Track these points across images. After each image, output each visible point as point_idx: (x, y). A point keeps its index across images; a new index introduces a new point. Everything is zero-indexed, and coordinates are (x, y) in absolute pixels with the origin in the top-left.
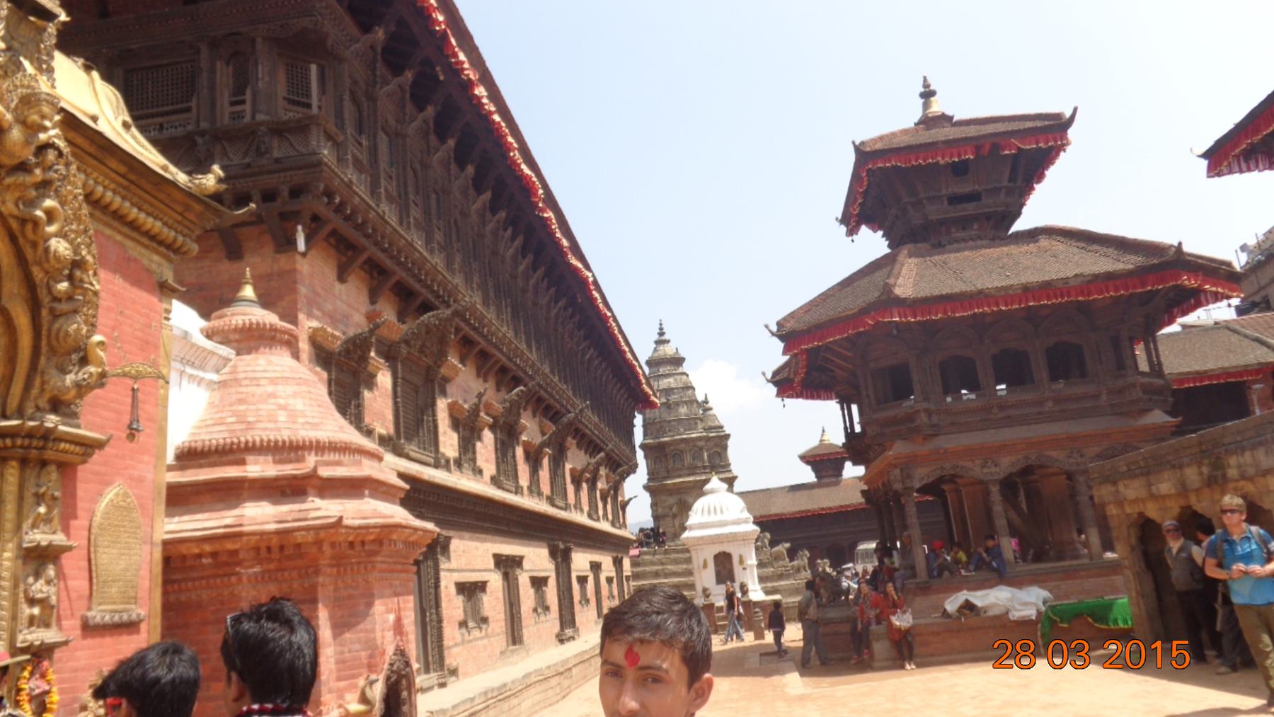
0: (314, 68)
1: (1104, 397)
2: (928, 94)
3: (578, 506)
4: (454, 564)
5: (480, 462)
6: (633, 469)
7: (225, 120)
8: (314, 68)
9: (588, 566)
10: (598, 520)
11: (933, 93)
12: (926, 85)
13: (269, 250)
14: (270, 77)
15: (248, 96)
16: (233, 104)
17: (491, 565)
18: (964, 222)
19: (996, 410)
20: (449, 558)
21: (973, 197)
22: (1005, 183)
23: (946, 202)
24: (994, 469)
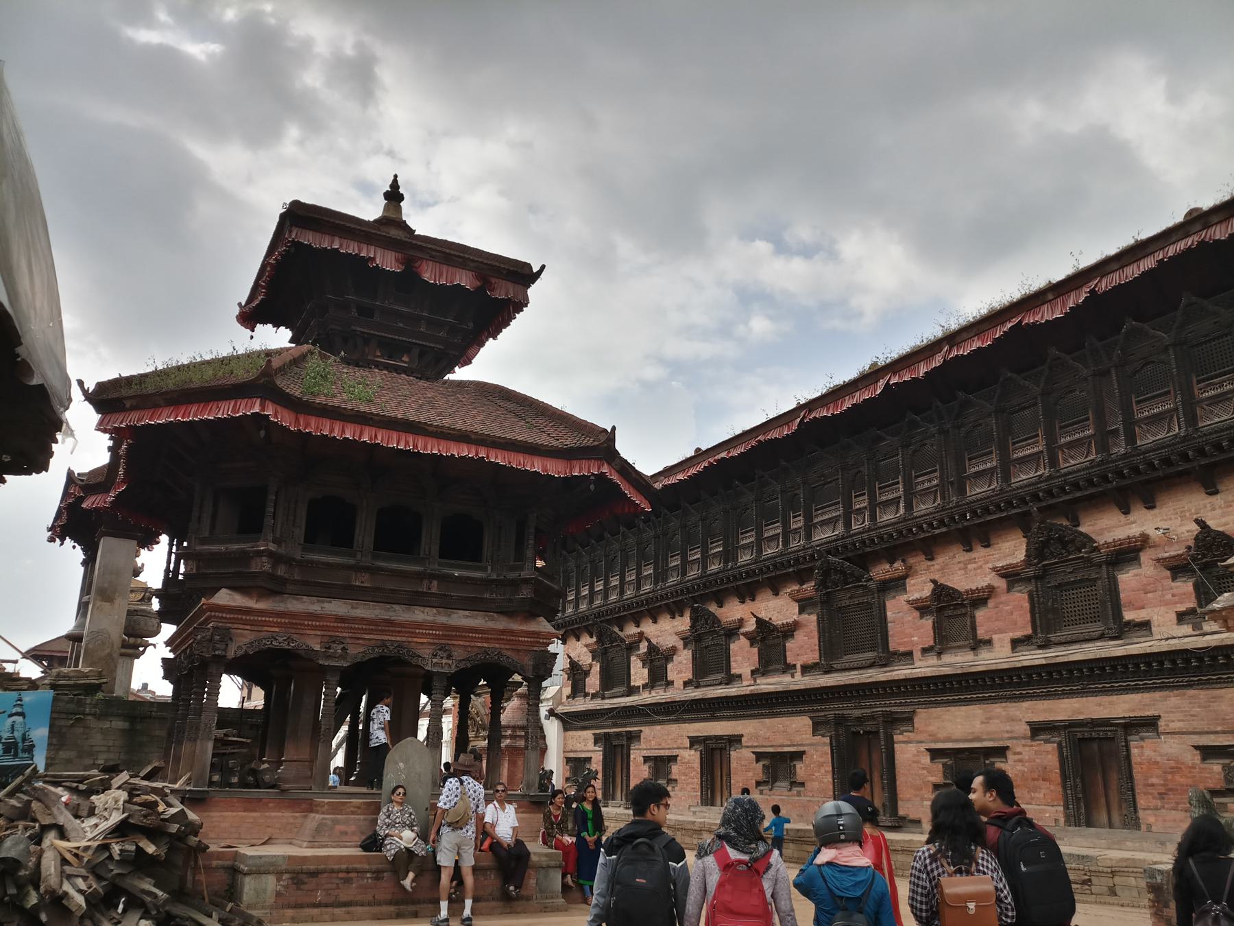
2: (394, 196)
4: (643, 746)
12: (395, 185)
17: (687, 743)
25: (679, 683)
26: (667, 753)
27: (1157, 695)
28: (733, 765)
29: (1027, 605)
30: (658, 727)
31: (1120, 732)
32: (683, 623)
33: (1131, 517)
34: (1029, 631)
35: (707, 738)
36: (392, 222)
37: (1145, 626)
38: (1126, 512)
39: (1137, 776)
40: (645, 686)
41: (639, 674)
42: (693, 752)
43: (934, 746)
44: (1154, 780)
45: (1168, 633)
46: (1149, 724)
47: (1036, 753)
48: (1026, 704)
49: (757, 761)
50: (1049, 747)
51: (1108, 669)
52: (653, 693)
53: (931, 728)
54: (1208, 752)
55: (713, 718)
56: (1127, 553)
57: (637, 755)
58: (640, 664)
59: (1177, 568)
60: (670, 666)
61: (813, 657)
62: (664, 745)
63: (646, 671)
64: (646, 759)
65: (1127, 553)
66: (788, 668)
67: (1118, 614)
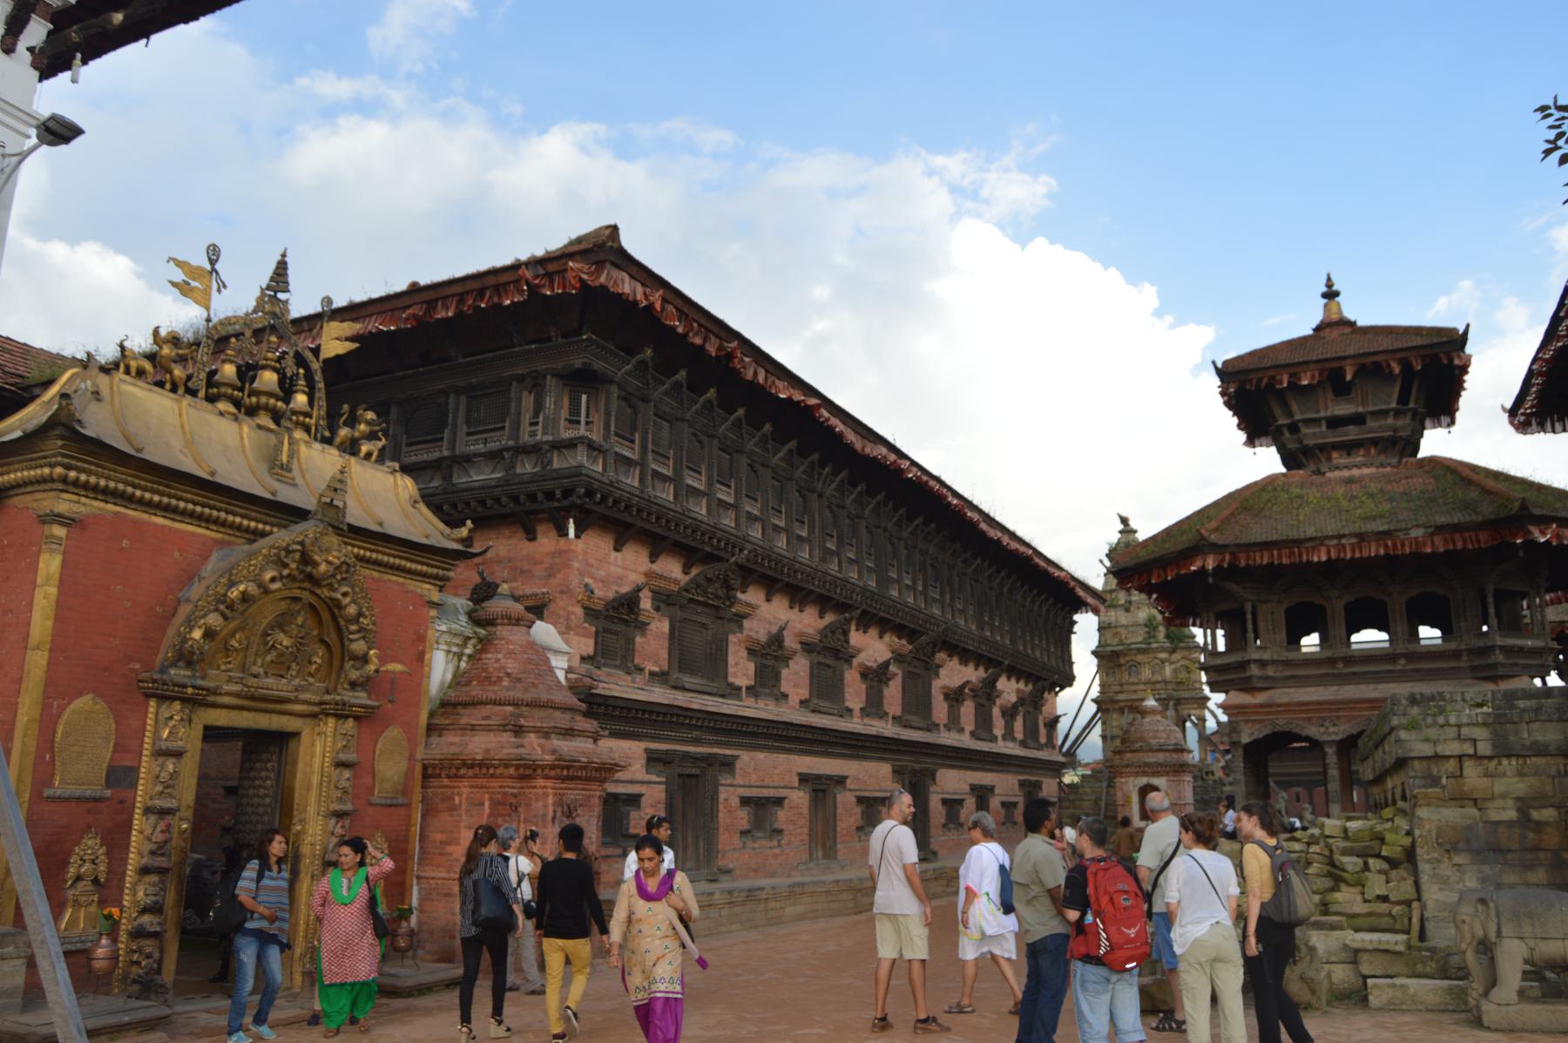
0: (584, 397)
1: (1464, 658)
2: (1331, 295)
3: (954, 723)
4: (739, 780)
5: (785, 687)
6: (1068, 680)
7: (526, 438)
8: (584, 397)
9: (967, 789)
10: (993, 739)
11: (1337, 294)
13: (553, 534)
14: (555, 402)
15: (541, 419)
16: (532, 424)
18: (1348, 447)
19: (1340, 665)
20: (733, 775)
21: (1358, 420)
22: (1394, 405)
23: (1324, 428)
24: (1331, 730)
25: (794, 700)
26: (771, 793)
28: (839, 810)
30: (761, 755)
35: (819, 777)
36: (1333, 325)
40: (748, 688)
41: (741, 670)
42: (801, 794)
52: (761, 704)
57: (728, 795)
58: (744, 653)
60: (785, 672)
61: (898, 713)
63: (751, 666)
66: (883, 715)
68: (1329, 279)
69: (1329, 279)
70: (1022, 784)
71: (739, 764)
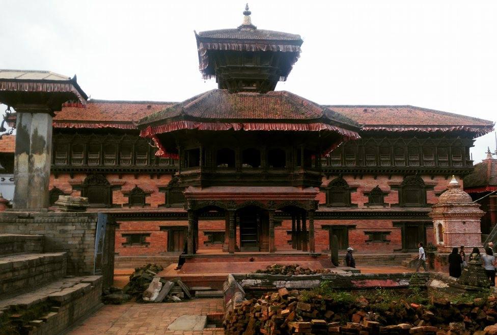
17: (159, 229)
20: (119, 228)
27: (356, 220)
29: (325, 196)
31: (346, 228)
32: (165, 181)
33: (356, 180)
34: (325, 202)
37: (356, 205)
38: (355, 178)
39: (350, 238)
40: (125, 205)
42: (162, 232)
43: (288, 230)
44: (353, 239)
45: (361, 208)
46: (353, 227)
47: (323, 233)
48: (321, 221)
49: (205, 235)
50: (327, 231)
51: (335, 214)
52: (133, 208)
53: (288, 225)
54: (366, 233)
55: (178, 220)
56: (354, 188)
59: (366, 194)
62: (139, 229)
64: (123, 235)
65: (354, 188)
67: (350, 202)
68: (247, 6)
69: (247, 6)
70: (394, 224)
71: (121, 226)
